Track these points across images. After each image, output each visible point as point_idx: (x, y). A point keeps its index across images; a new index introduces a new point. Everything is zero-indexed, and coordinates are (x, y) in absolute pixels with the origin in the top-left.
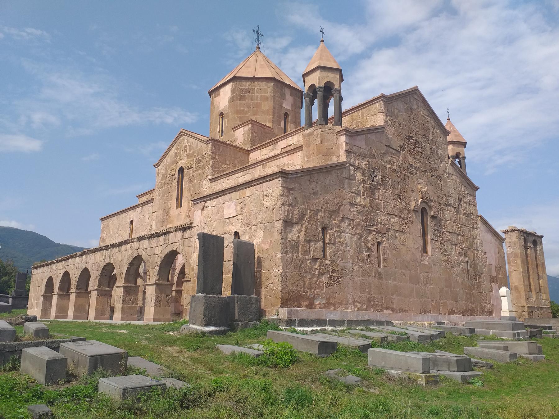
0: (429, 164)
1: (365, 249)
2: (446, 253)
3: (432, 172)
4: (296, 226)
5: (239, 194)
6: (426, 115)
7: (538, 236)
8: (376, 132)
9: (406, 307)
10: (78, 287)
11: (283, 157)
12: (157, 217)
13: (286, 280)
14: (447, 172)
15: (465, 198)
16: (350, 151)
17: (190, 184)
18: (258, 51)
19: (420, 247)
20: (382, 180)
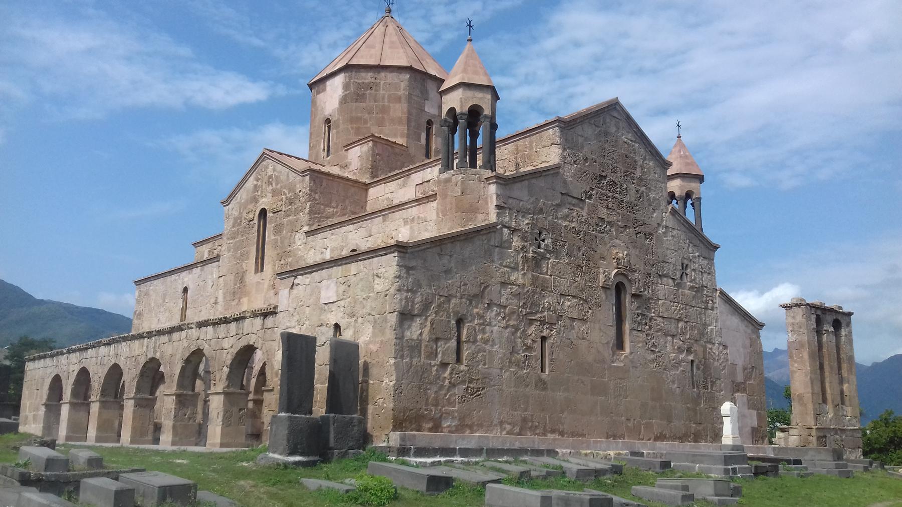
0: (632, 216)
1: (523, 347)
3: (636, 227)
4: (418, 319)
5: (341, 270)
6: (631, 141)
7: (844, 314)
8: (545, 176)
9: (583, 430)
10: (103, 393)
11: (412, 207)
12: (226, 284)
13: (400, 394)
14: (663, 226)
17: (277, 237)
18: (388, 16)
19: (611, 340)
20: (552, 245)
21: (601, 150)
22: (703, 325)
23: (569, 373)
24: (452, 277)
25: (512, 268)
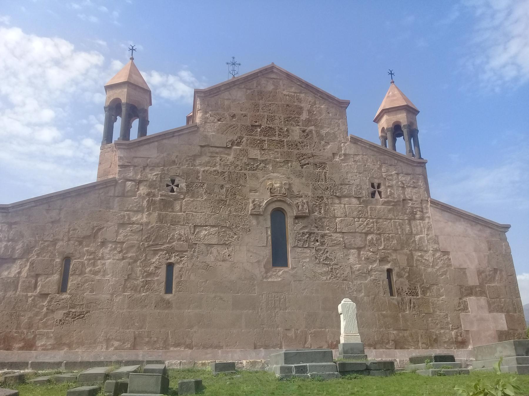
0: (296, 151)
1: (143, 274)
3: (302, 160)
4: (19, 262)
8: (180, 135)
9: (220, 342)
15: (391, 180)
16: (126, 165)
21: (253, 106)
22: (407, 234)
23: (202, 292)
24: (61, 225)
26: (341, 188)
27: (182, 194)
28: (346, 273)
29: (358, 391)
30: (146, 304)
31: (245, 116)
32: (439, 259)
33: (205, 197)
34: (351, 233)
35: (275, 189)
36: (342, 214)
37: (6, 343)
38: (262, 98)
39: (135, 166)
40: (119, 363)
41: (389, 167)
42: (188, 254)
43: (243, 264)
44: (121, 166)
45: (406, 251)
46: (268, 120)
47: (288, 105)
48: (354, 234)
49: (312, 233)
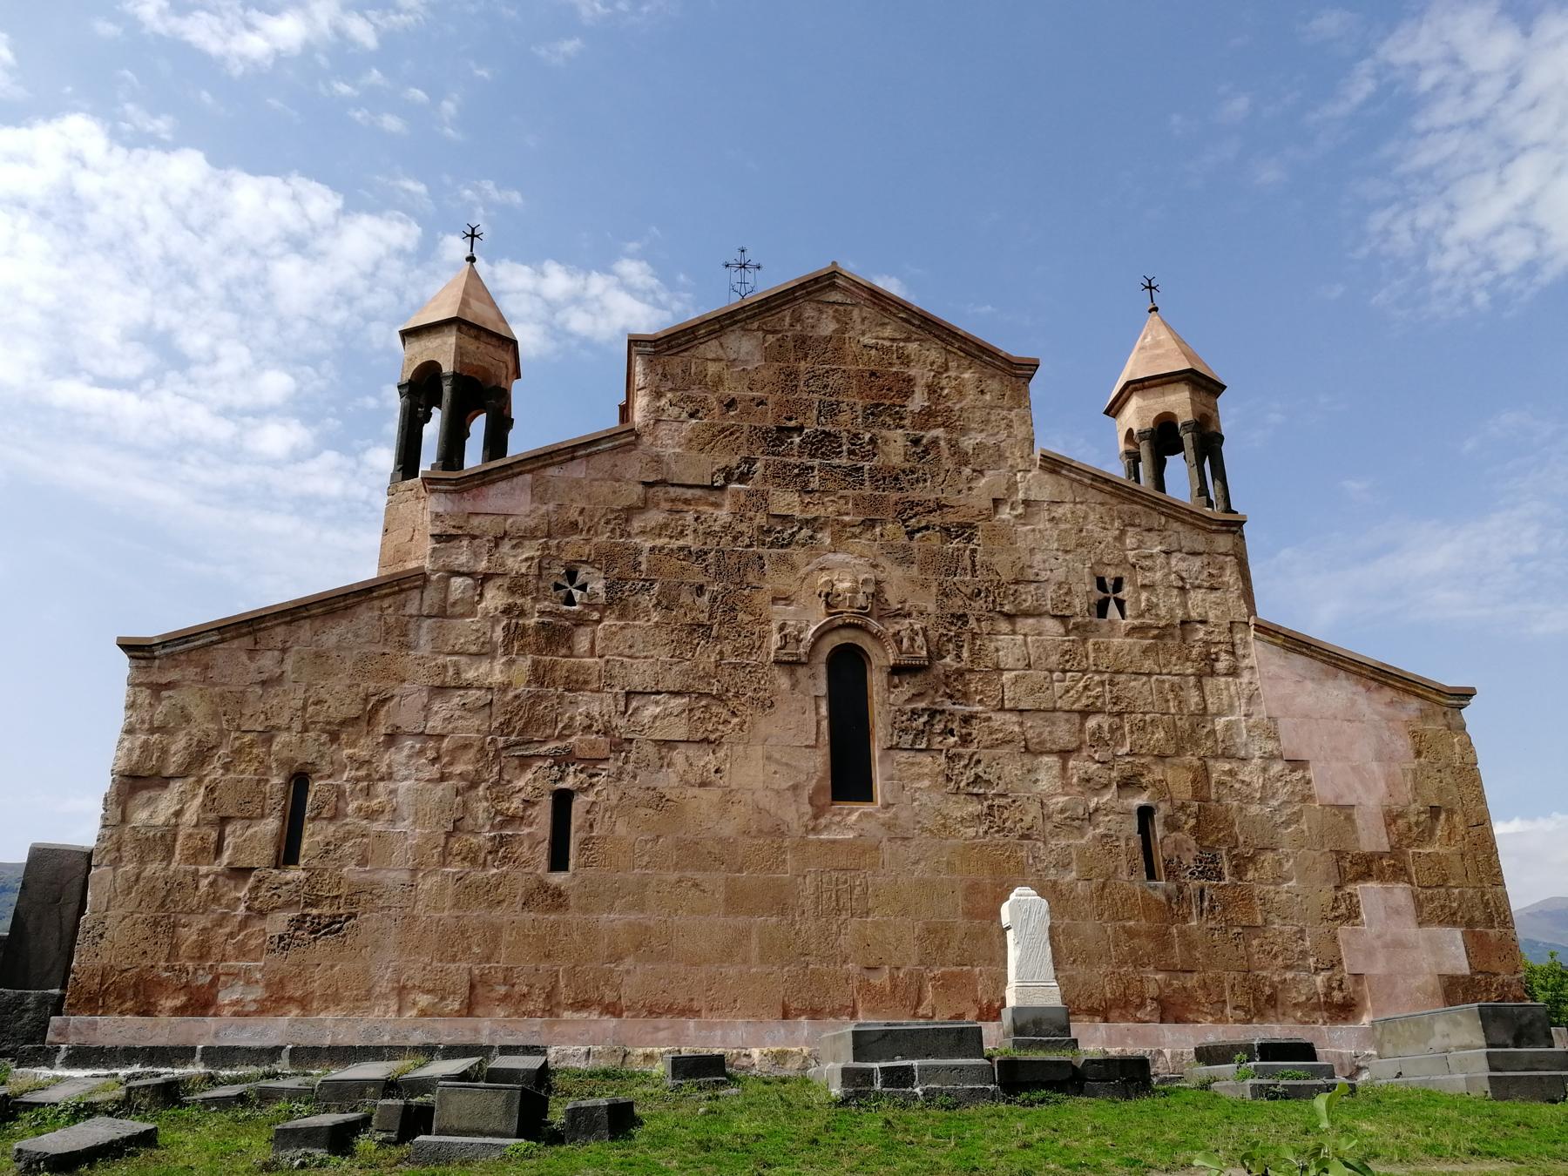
0: (895, 496)
1: (494, 818)
2: (975, 790)
3: (911, 518)
4: (178, 784)
8: (589, 455)
9: (692, 1000)
13: (97, 939)
15: (1150, 569)
16: (451, 535)
19: (809, 779)
21: (782, 377)
22: (1193, 715)
25: (476, 655)
26: (1016, 591)
27: (596, 610)
28: (1028, 819)
29: (1041, 1140)
30: (501, 898)
31: (761, 403)
32: (1279, 781)
33: (655, 617)
34: (1043, 711)
35: (839, 595)
36: (1018, 660)
37: (141, 997)
38: (806, 355)
39: (474, 537)
40: (429, 1052)
41: (1145, 533)
42: (612, 766)
43: (753, 793)
44: (438, 538)
45: (1189, 758)
46: (820, 412)
47: (873, 374)
48: (1048, 715)
49: (936, 711)
